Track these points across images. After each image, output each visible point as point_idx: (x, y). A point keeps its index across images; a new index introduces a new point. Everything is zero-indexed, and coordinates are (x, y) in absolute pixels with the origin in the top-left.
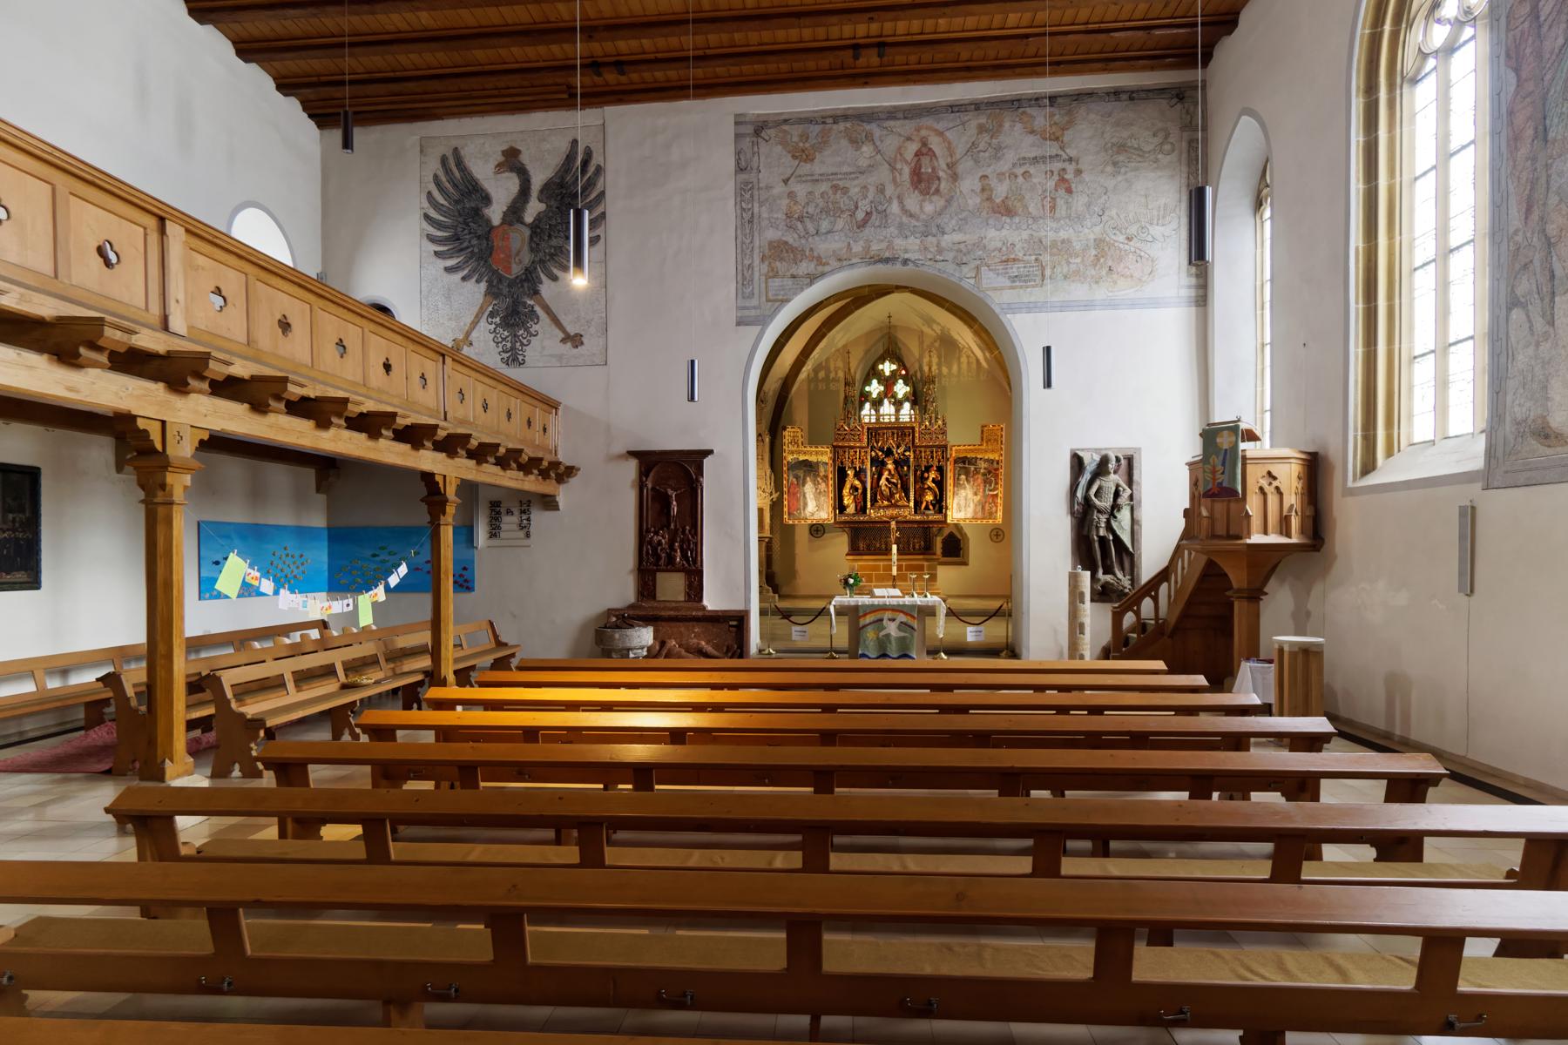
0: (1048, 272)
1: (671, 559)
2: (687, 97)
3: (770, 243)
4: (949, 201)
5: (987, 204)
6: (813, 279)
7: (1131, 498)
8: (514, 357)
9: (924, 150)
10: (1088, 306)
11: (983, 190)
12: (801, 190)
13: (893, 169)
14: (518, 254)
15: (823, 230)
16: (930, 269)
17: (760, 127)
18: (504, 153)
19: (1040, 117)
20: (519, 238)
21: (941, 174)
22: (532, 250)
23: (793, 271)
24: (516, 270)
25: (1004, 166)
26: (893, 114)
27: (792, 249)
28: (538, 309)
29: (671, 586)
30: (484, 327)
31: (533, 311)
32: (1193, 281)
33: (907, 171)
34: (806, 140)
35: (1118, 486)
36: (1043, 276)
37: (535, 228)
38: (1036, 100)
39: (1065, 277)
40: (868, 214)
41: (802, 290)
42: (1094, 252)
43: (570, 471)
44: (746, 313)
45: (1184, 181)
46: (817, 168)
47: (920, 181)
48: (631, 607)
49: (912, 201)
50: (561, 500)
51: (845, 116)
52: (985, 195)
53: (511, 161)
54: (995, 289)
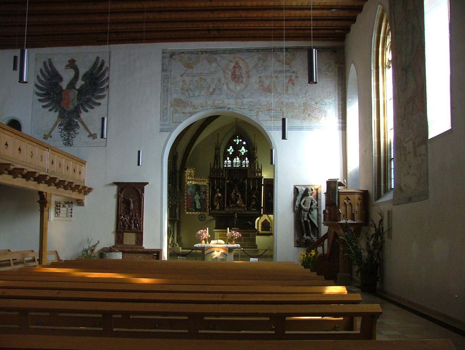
1: (130, 227)
2: (143, 42)
3: (175, 99)
4: (246, 86)
6: (191, 114)
7: (317, 205)
8: (68, 143)
9: (237, 66)
10: (301, 128)
11: (260, 82)
12: (187, 79)
13: (224, 73)
14: (72, 101)
17: (172, 54)
18: (69, 61)
19: (283, 56)
20: (73, 95)
21: (243, 75)
22: (78, 99)
23: (184, 111)
24: (71, 107)
26: (224, 51)
28: (79, 123)
29: (130, 239)
30: (57, 129)
31: (77, 125)
32: (341, 120)
33: (230, 73)
35: (312, 200)
37: (80, 91)
38: (281, 49)
41: (187, 118)
42: (303, 108)
43: (90, 190)
44: (164, 127)
47: (235, 78)
48: (113, 247)
50: (85, 202)
53: (72, 64)
54: (264, 121)
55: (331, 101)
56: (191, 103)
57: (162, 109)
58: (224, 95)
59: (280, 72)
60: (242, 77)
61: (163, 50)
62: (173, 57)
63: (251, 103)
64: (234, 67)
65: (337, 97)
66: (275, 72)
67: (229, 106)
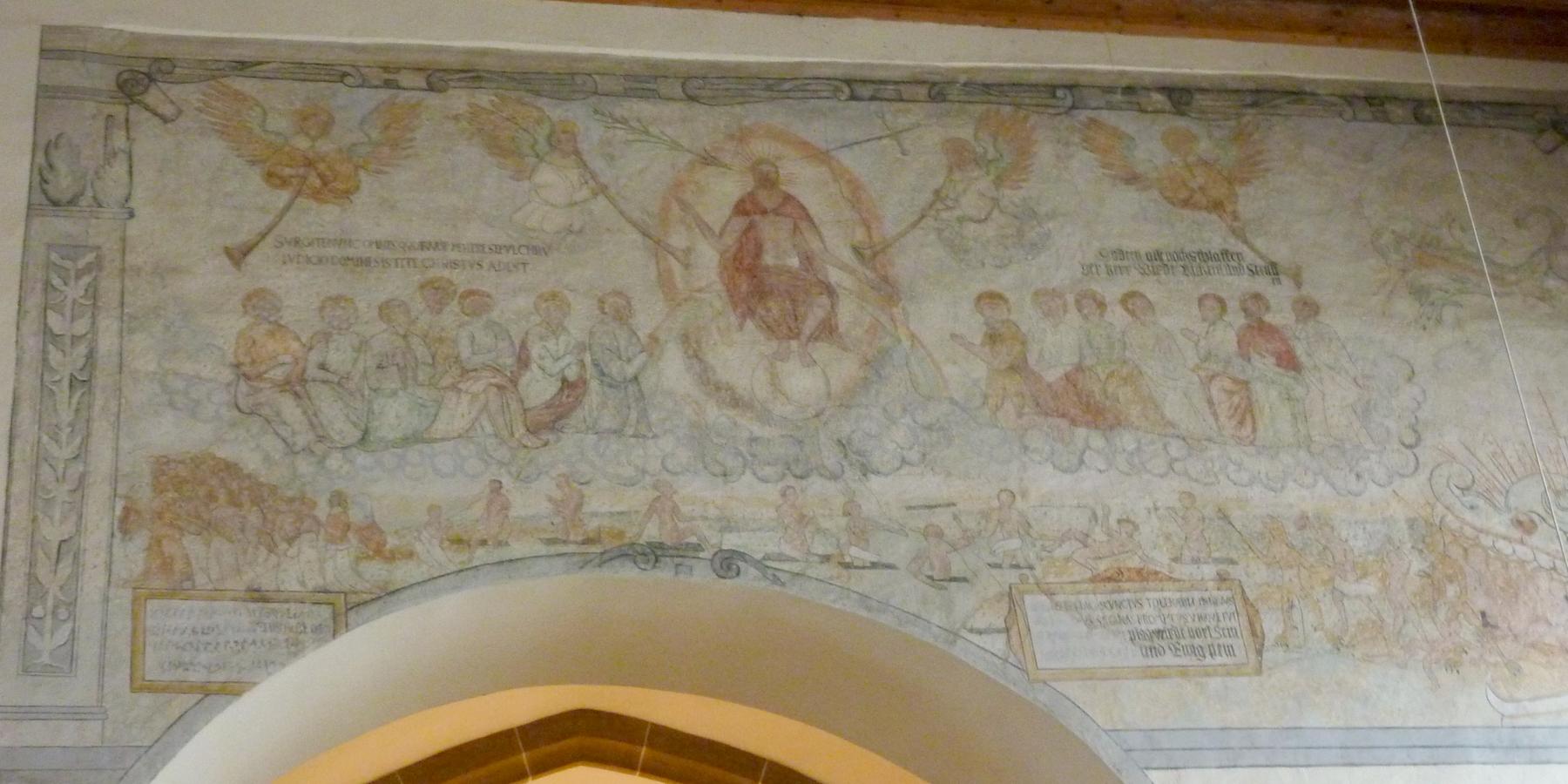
0: (1271, 625)
4: (874, 365)
6: (342, 609)
9: (767, 200)
11: (993, 338)
12: (299, 290)
13: (658, 246)
19: (1149, 141)
21: (835, 276)
25: (1060, 264)
26: (644, 81)
27: (260, 494)
33: (709, 257)
36: (1256, 634)
38: (1131, 92)
39: (1338, 644)
40: (571, 388)
41: (296, 648)
42: (1417, 565)
47: (761, 292)
49: (740, 355)
54: (1087, 675)
56: (338, 499)
58: (667, 444)
59: (1157, 261)
60: (830, 290)
61: (47, 30)
62: (153, 97)
63: (942, 518)
64: (741, 209)
67: (731, 541)
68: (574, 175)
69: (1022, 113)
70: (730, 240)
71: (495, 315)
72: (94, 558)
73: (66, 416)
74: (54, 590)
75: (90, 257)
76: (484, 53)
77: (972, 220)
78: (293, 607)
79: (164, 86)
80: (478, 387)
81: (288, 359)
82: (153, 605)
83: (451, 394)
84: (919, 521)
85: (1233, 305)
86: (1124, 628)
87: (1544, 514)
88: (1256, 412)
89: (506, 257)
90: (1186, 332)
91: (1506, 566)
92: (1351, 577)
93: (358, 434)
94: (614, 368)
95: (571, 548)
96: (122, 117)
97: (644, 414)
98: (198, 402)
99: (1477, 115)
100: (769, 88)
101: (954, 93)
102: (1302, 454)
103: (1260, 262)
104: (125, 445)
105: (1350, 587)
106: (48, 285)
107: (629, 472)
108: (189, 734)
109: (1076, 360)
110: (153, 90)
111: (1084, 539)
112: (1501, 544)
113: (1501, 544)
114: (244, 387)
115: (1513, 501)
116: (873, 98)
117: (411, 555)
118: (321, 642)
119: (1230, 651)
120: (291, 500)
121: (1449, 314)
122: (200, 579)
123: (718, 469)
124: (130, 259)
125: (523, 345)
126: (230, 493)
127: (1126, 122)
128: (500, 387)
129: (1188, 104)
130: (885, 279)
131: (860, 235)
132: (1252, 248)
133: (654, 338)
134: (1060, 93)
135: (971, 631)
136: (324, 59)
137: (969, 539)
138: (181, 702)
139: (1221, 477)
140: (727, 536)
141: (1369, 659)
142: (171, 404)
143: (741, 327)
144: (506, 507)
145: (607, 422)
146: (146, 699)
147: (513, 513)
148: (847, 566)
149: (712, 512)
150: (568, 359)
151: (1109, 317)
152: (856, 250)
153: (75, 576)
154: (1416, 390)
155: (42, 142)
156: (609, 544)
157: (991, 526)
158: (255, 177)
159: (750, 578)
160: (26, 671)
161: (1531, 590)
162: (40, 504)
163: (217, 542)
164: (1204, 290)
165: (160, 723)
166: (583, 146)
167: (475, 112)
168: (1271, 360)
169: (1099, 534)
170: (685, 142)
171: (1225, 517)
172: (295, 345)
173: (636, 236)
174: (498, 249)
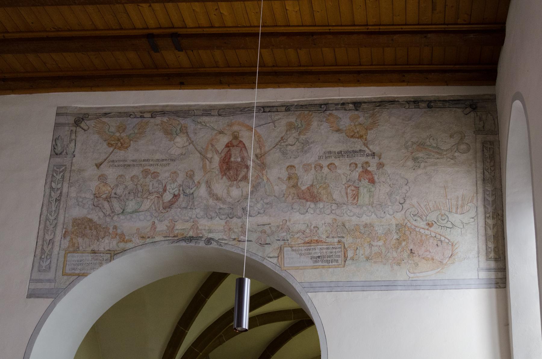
0: (350, 254)
5: (293, 191)
6: (113, 255)
9: (235, 143)
10: (389, 286)
11: (289, 178)
12: (111, 173)
13: (204, 157)
15: (129, 209)
16: (231, 248)
17: (80, 119)
19: (345, 119)
23: (95, 247)
26: (207, 111)
32: (492, 264)
33: (217, 159)
34: (122, 131)
36: (346, 257)
38: (343, 105)
40: (176, 197)
41: (101, 264)
44: (39, 286)
45: (480, 175)
46: (130, 155)
47: (229, 169)
49: (220, 186)
51: (163, 112)
52: (292, 182)
54: (297, 268)
55: (466, 218)
56: (115, 228)
57: (40, 243)
58: (198, 210)
61: (58, 108)
62: (83, 125)
63: (266, 228)
64: (227, 146)
65: (481, 209)
66: (329, 154)
67: (211, 236)
68: (185, 139)
69: (311, 113)
70: (223, 155)
71: (159, 178)
72: (57, 244)
73: (54, 209)
74: (47, 251)
75: (64, 168)
76: (167, 106)
77: (290, 145)
78: (101, 254)
79: (86, 121)
80: (152, 197)
81: (107, 192)
82: (69, 254)
83: (146, 200)
84: (260, 229)
85: (359, 165)
86: (310, 256)
87: (436, 221)
88: (359, 195)
89: (164, 162)
90: (344, 174)
91: (422, 236)
92: (376, 241)
93: (122, 211)
94: (187, 191)
95: (170, 238)
96: (74, 130)
97: (193, 203)
98: (84, 204)
99: (447, 104)
100: (241, 111)
101: (293, 108)
102: (370, 207)
103: (370, 153)
104: (67, 215)
105: (374, 243)
106: (53, 175)
107: (188, 218)
108: (74, 286)
109: (311, 183)
110: (83, 122)
111: (304, 232)
112: (422, 231)
113: (422, 231)
114: (96, 199)
115: (428, 218)
116: (269, 112)
117: (131, 241)
118: (107, 263)
119: (337, 261)
120: (104, 228)
121: (422, 165)
122: (81, 248)
123: (210, 217)
124: (73, 168)
125: (165, 186)
126: (90, 227)
127: (339, 114)
128: (158, 197)
129: (360, 107)
130: (263, 163)
131: (258, 151)
132: (369, 149)
133: (199, 182)
134: (323, 106)
135: (268, 257)
136: (126, 111)
137: (273, 233)
138: (75, 277)
139: (345, 214)
140: (210, 234)
141: (375, 262)
142: (78, 205)
143: (222, 178)
144: (155, 228)
145: (184, 205)
146: (65, 277)
147: (157, 230)
148: (239, 241)
149: (207, 228)
150: (176, 189)
151: (323, 171)
152: (256, 156)
153: (52, 248)
154: (408, 187)
155: (54, 138)
156: (180, 237)
157: (279, 230)
158: (105, 145)
159: (214, 245)
160: (39, 271)
161: (427, 243)
162: (46, 231)
163: (86, 239)
164: (352, 161)
165: (68, 283)
166: (189, 131)
167: (162, 122)
168: (367, 181)
169: (308, 231)
170: (216, 127)
171: (344, 225)
172: (110, 188)
173: (199, 155)
174: (163, 160)
